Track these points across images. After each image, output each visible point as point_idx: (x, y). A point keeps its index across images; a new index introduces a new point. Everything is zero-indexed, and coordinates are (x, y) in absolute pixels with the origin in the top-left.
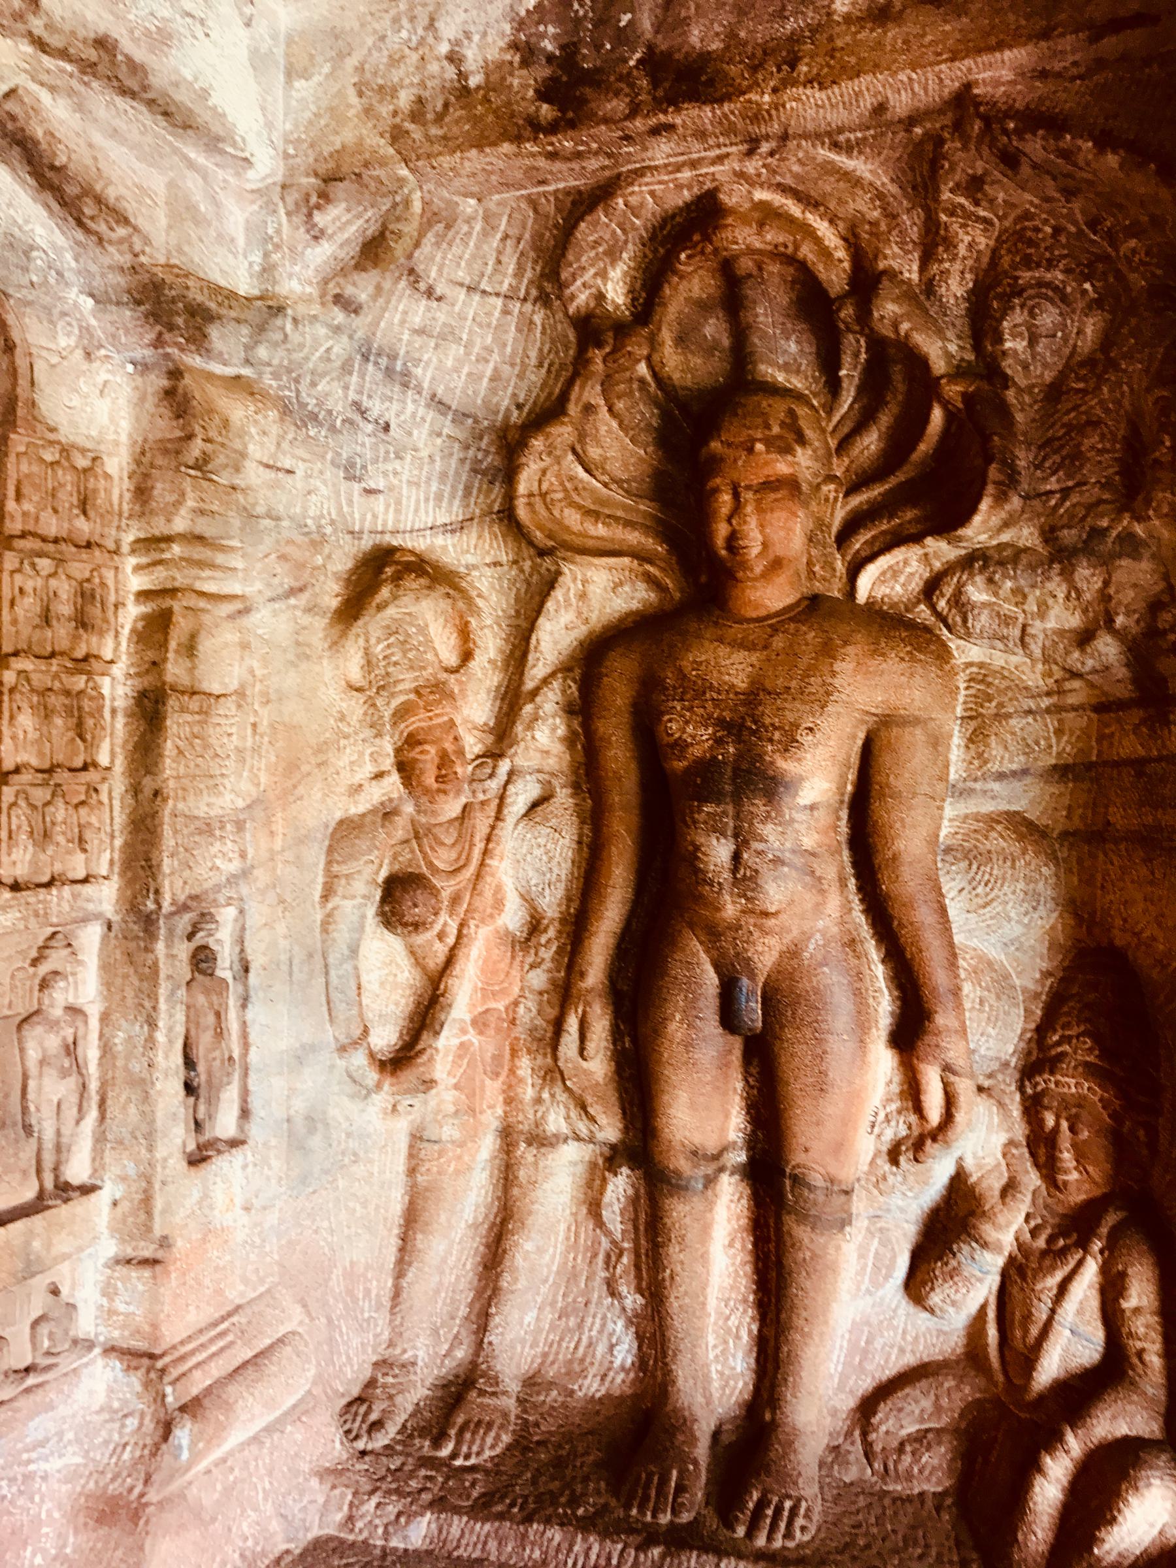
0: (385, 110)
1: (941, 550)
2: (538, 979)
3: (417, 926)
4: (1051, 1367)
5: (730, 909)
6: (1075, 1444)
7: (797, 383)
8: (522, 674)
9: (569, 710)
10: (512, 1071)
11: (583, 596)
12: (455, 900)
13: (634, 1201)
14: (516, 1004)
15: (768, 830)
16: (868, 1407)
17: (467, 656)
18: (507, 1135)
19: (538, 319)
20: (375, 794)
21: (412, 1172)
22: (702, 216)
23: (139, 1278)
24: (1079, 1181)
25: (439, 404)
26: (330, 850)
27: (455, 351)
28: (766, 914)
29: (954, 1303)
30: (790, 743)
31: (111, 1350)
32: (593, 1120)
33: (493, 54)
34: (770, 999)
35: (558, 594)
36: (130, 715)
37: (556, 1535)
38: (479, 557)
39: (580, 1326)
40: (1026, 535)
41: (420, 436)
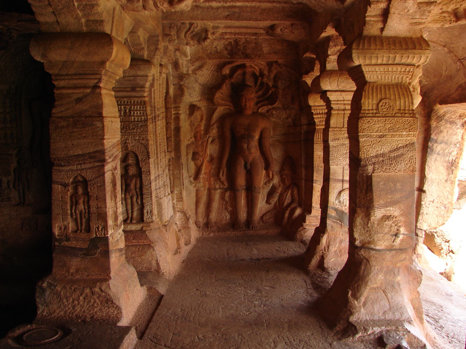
0: (206, 53)
1: (270, 107)
2: (214, 166)
3: (198, 160)
4: (286, 203)
5: (247, 152)
6: (289, 209)
7: (251, 85)
8: (210, 122)
9: (218, 127)
10: (210, 180)
11: (220, 111)
12: (202, 156)
13: (230, 195)
14: (210, 171)
15: (252, 143)
16: (262, 218)
17: (202, 120)
18: (209, 190)
19: (216, 74)
20: (191, 140)
21: (197, 195)
22: (243, 66)
23: (181, 203)
24: (287, 183)
25: (200, 84)
26: (187, 149)
27: (204, 77)
28: (251, 153)
29: (273, 201)
30: (254, 131)
31: (178, 211)
32: (225, 185)
33: (221, 48)
34: (250, 165)
35: (217, 111)
36: (174, 130)
37: (229, 232)
38: (203, 105)
39: (221, 215)
40: (280, 106)
41: (197, 88)
